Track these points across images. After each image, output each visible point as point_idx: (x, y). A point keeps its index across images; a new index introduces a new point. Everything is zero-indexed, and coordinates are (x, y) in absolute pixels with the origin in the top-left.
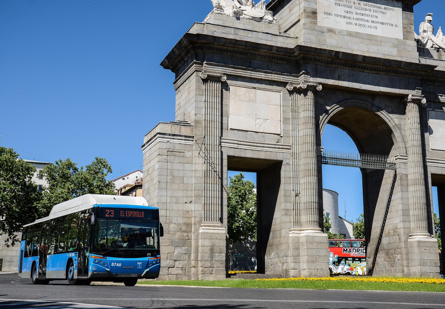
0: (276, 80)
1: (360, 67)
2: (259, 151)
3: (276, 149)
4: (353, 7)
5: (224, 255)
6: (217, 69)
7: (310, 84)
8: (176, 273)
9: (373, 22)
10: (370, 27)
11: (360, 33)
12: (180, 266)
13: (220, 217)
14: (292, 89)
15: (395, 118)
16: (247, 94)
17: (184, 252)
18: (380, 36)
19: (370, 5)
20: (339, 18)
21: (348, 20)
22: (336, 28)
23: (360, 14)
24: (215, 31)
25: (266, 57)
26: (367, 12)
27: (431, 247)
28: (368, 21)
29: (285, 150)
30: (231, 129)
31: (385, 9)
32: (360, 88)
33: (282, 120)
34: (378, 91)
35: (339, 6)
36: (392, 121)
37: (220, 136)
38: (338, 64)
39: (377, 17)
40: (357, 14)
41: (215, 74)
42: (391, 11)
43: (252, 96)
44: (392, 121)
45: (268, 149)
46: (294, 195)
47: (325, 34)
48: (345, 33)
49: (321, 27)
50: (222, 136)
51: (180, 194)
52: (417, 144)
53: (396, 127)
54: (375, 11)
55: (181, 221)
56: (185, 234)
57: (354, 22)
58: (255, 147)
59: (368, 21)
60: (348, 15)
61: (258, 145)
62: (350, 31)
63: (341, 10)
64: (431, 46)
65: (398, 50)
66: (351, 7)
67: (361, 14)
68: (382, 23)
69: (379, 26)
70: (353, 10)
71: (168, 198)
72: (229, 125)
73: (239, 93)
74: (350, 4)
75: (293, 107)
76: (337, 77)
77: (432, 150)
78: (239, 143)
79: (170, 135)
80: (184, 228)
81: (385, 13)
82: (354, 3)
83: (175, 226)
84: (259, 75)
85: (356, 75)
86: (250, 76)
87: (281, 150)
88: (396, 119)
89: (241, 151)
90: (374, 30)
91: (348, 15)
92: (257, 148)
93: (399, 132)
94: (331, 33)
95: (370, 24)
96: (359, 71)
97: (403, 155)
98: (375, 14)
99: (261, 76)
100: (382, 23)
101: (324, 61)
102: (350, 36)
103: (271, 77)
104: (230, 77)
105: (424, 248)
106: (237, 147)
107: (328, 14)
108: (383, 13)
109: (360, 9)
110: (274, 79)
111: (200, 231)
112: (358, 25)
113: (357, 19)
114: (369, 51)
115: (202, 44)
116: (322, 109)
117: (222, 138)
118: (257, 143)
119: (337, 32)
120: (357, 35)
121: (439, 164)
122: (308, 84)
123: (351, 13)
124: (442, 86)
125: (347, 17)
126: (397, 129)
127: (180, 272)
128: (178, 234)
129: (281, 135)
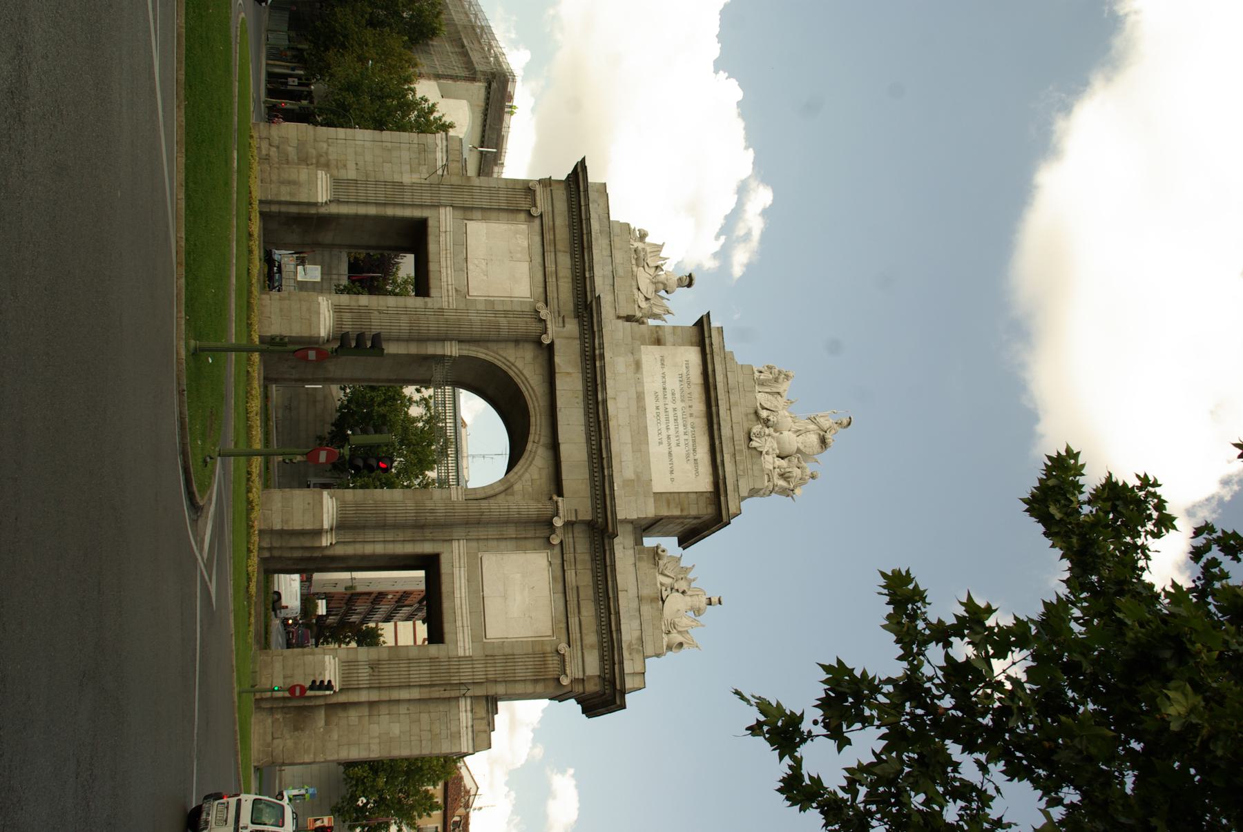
3: (446, 286)
4: (683, 405)
5: (288, 198)
6: (546, 206)
8: (262, 147)
9: (669, 437)
11: (645, 414)
12: (271, 153)
13: (341, 200)
16: (519, 249)
17: (290, 159)
20: (659, 379)
21: (661, 395)
22: (644, 373)
23: (675, 415)
26: (681, 429)
27: (314, 516)
28: (668, 429)
29: (446, 299)
30: (466, 224)
32: (558, 409)
33: (490, 298)
34: (560, 441)
35: (680, 381)
36: (516, 477)
39: (678, 445)
40: (675, 409)
42: (694, 472)
43: (519, 255)
44: (516, 477)
45: (445, 274)
46: (379, 308)
47: (630, 355)
49: (640, 350)
51: (369, 158)
55: (332, 157)
56: (314, 161)
57: (661, 404)
58: (444, 256)
59: (668, 429)
60: (669, 396)
63: (673, 384)
65: (633, 480)
66: (682, 401)
68: (670, 453)
69: (664, 449)
70: (679, 405)
71: (362, 143)
77: (481, 558)
79: (447, 146)
80: (323, 160)
82: (690, 407)
83: (324, 150)
85: (578, 403)
87: (446, 293)
88: (521, 487)
90: (657, 439)
91: (669, 396)
92: (444, 259)
94: (633, 366)
95: (664, 434)
98: (682, 443)
100: (670, 453)
102: (638, 397)
103: (550, 280)
105: (311, 502)
108: (688, 456)
109: (684, 416)
111: (319, 172)
112: (657, 411)
114: (621, 427)
116: (516, 358)
119: (638, 376)
120: (642, 408)
123: (674, 401)
126: (506, 486)
127: (264, 152)
128: (313, 152)
129: (468, 297)
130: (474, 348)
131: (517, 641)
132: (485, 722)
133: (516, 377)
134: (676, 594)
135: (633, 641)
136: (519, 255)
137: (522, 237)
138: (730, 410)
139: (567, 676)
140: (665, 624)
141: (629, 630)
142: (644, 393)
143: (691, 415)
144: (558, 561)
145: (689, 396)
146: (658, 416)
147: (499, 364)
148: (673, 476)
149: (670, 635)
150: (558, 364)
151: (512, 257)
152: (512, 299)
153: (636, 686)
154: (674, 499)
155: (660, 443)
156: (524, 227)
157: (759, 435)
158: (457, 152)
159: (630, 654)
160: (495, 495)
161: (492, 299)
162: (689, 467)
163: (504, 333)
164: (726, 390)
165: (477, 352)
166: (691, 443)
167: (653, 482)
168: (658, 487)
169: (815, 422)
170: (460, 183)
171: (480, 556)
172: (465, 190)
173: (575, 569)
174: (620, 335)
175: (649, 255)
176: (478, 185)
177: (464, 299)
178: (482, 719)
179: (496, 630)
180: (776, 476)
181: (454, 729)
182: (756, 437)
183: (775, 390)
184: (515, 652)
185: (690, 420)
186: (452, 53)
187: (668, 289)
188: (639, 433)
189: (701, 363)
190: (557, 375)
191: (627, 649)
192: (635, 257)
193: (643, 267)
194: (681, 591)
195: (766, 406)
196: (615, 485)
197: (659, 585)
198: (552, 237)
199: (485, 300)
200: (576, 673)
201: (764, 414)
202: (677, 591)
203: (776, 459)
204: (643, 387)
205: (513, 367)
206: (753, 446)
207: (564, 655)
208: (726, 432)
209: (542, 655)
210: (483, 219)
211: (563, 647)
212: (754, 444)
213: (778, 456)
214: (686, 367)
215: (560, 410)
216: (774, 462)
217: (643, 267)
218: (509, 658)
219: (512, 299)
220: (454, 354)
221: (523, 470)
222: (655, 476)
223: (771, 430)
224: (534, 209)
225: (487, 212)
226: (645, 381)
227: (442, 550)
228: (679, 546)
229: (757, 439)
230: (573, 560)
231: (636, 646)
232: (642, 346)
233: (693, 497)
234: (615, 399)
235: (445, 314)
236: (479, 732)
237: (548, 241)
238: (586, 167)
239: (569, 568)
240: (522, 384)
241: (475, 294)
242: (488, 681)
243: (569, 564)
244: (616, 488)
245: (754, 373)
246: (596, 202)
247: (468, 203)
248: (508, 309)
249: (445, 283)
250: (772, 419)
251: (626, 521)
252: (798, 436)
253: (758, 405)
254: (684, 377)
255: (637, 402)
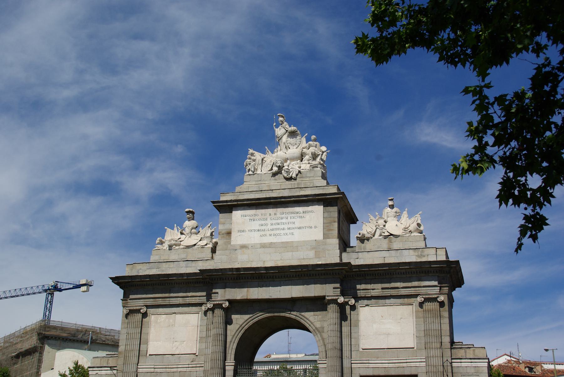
0: (193, 302)
1: (267, 277)
2: (174, 372)
3: (190, 368)
4: (269, 219)
6: (140, 303)
7: (215, 303)
9: (289, 229)
10: (285, 234)
11: (274, 243)
14: (207, 309)
15: (318, 321)
18: (296, 241)
19: (287, 213)
20: (253, 233)
24: (141, 269)
25: (182, 284)
26: (284, 221)
28: (284, 229)
29: (198, 368)
30: (150, 355)
31: (303, 213)
32: (271, 298)
34: (290, 297)
35: (254, 221)
36: (312, 325)
37: (137, 363)
38: (245, 278)
39: (294, 223)
40: (272, 224)
41: (135, 308)
43: (171, 321)
45: (182, 369)
47: (237, 252)
48: (259, 246)
49: (234, 245)
50: (138, 363)
52: (331, 347)
53: (316, 331)
54: (292, 218)
57: (268, 233)
58: (170, 369)
59: (284, 229)
60: (263, 228)
61: (172, 367)
62: (263, 243)
63: (255, 225)
64: (379, 235)
65: (315, 251)
67: (277, 224)
68: (299, 228)
69: (296, 232)
70: (269, 222)
72: (148, 351)
73: (160, 320)
74: (265, 217)
75: (208, 326)
76: (246, 291)
78: (155, 367)
79: (98, 367)
81: (303, 217)
82: (270, 215)
84: (176, 301)
86: (169, 303)
88: (318, 322)
89: (157, 375)
91: (263, 228)
92: (172, 369)
93: (319, 336)
94: (244, 249)
95: (287, 231)
96: (269, 281)
97: (322, 359)
99: (179, 301)
100: (299, 228)
101: (230, 279)
102: (264, 247)
103: (188, 301)
104: (148, 307)
106: (153, 371)
107: (242, 231)
108: (301, 217)
110: (191, 303)
112: (272, 235)
113: (272, 229)
115: (126, 283)
117: (139, 364)
118: (171, 365)
119: (250, 247)
120: (271, 245)
121: (370, 365)
122: (213, 303)
123: (266, 225)
124: (375, 279)
125: (261, 230)
126: (318, 332)
129: (196, 355)
130: (230, 351)
131: (416, 328)
132: (468, 350)
133: (249, 324)
134: (386, 226)
135: (416, 254)
136: (171, 321)
137: (159, 318)
138: (272, 190)
139: (438, 297)
140: (406, 234)
141: (410, 257)
142: (261, 243)
143: (275, 214)
144: (366, 302)
145: (263, 215)
146: (275, 235)
147: (240, 335)
148: (313, 226)
149: (412, 231)
150: (243, 296)
151: (172, 325)
152: (199, 325)
153: (444, 253)
154: (328, 226)
155: (292, 234)
156: (153, 318)
157: (288, 172)
158: (102, 360)
159: (424, 256)
160: (323, 339)
161: (198, 339)
162: (307, 216)
163: (221, 331)
164: (260, 192)
165: (232, 348)
166: (293, 215)
167: (317, 239)
168: (320, 236)
169: (281, 137)
170: (123, 358)
171: (362, 350)
172: (127, 355)
173: (370, 289)
174: (224, 258)
175: (173, 238)
176: (124, 346)
177: (198, 357)
178: (466, 352)
179: (410, 342)
180: (314, 163)
181: (473, 371)
182: (289, 175)
183: (260, 162)
184: (423, 329)
185: (279, 215)
186: (22, 363)
187: (195, 226)
188: (286, 247)
189: (243, 207)
190: (249, 298)
191: (421, 258)
192: (174, 246)
193: (181, 241)
194: (385, 224)
195: (270, 168)
196: (318, 263)
197: (381, 237)
198: (160, 299)
199: (199, 343)
200: (436, 291)
201: (275, 169)
202: (384, 226)
203: (303, 162)
204: (257, 244)
205: (243, 326)
206: (295, 177)
207: (425, 299)
208: (286, 193)
209: (425, 312)
210: (147, 343)
211: (420, 299)
212: (294, 176)
213: (302, 161)
214: (246, 216)
215: (270, 296)
216: (305, 163)
217: (181, 241)
218: (427, 333)
219: (199, 325)
220: (234, 364)
221: (307, 321)
222: (313, 238)
223: (285, 164)
224: (141, 311)
225: (142, 340)
226: (253, 243)
227: (358, 374)
228: (356, 223)
229: (291, 174)
230: (365, 291)
231: (419, 252)
232: (232, 244)
233: (326, 215)
234: (264, 262)
235: (207, 369)
236: (474, 354)
237: (163, 302)
238: (116, 277)
239: (369, 293)
240: (254, 320)
241: (195, 349)
242: (441, 347)
243: (367, 294)
244: (320, 263)
245: (250, 175)
246: (138, 270)
247: (136, 354)
248: (206, 328)
249: (188, 369)
250: (279, 164)
251: (341, 257)
252: (289, 148)
253: (270, 172)
254: (252, 218)
255: (266, 248)
